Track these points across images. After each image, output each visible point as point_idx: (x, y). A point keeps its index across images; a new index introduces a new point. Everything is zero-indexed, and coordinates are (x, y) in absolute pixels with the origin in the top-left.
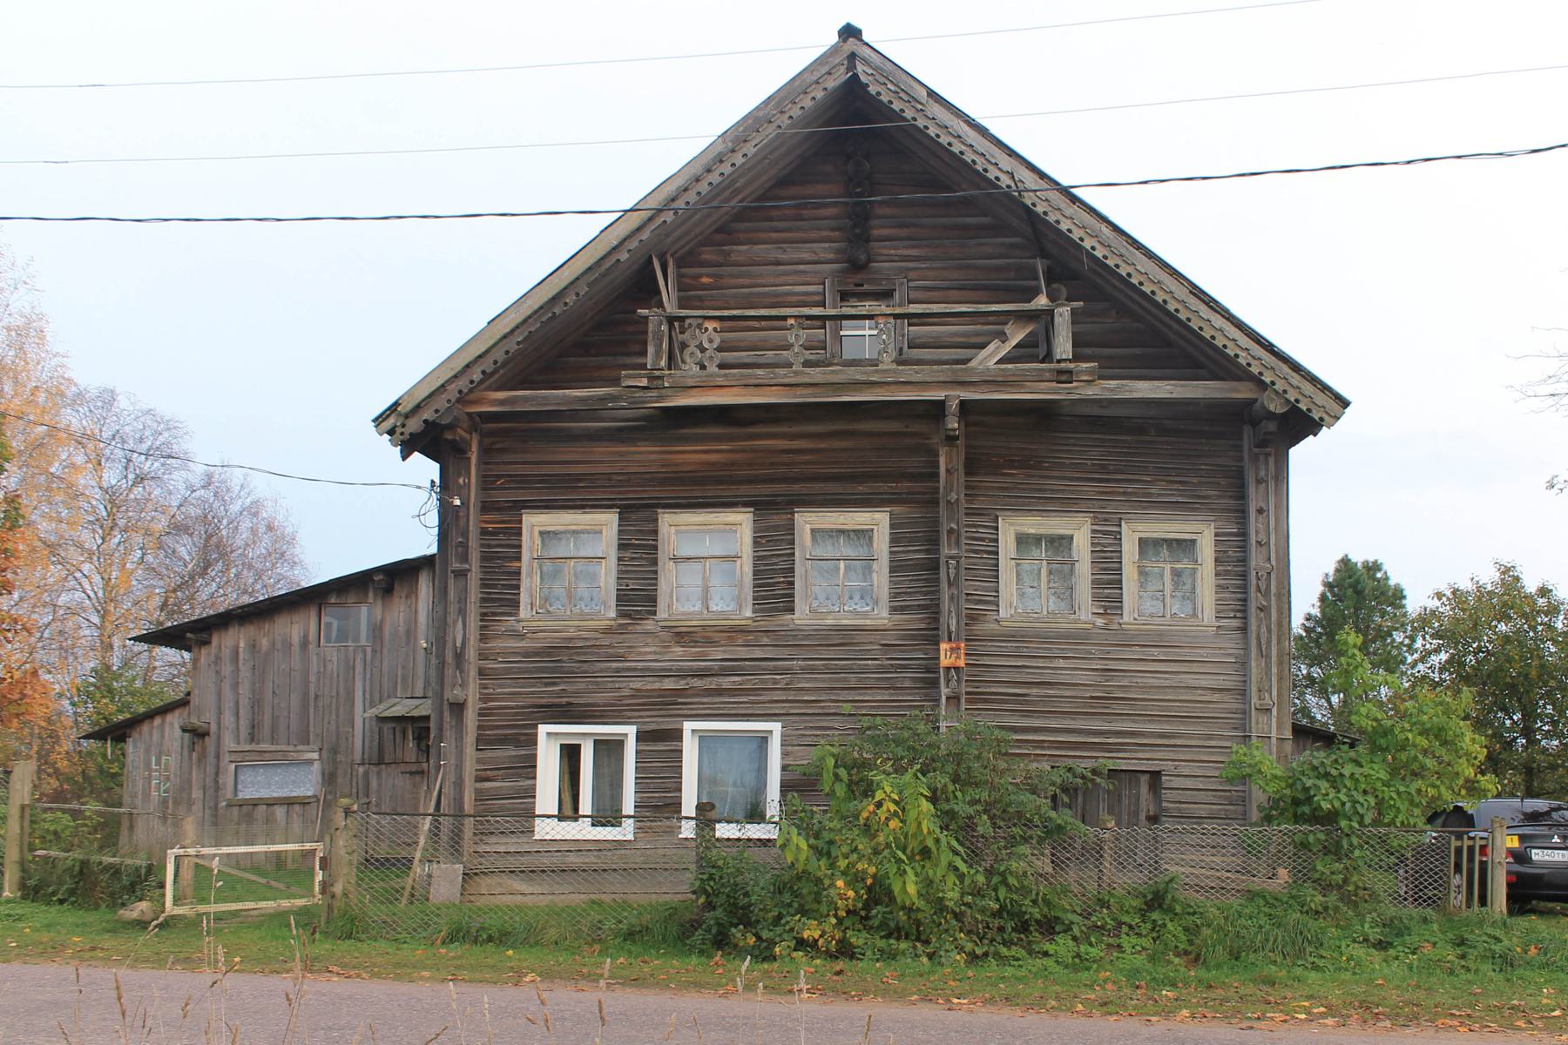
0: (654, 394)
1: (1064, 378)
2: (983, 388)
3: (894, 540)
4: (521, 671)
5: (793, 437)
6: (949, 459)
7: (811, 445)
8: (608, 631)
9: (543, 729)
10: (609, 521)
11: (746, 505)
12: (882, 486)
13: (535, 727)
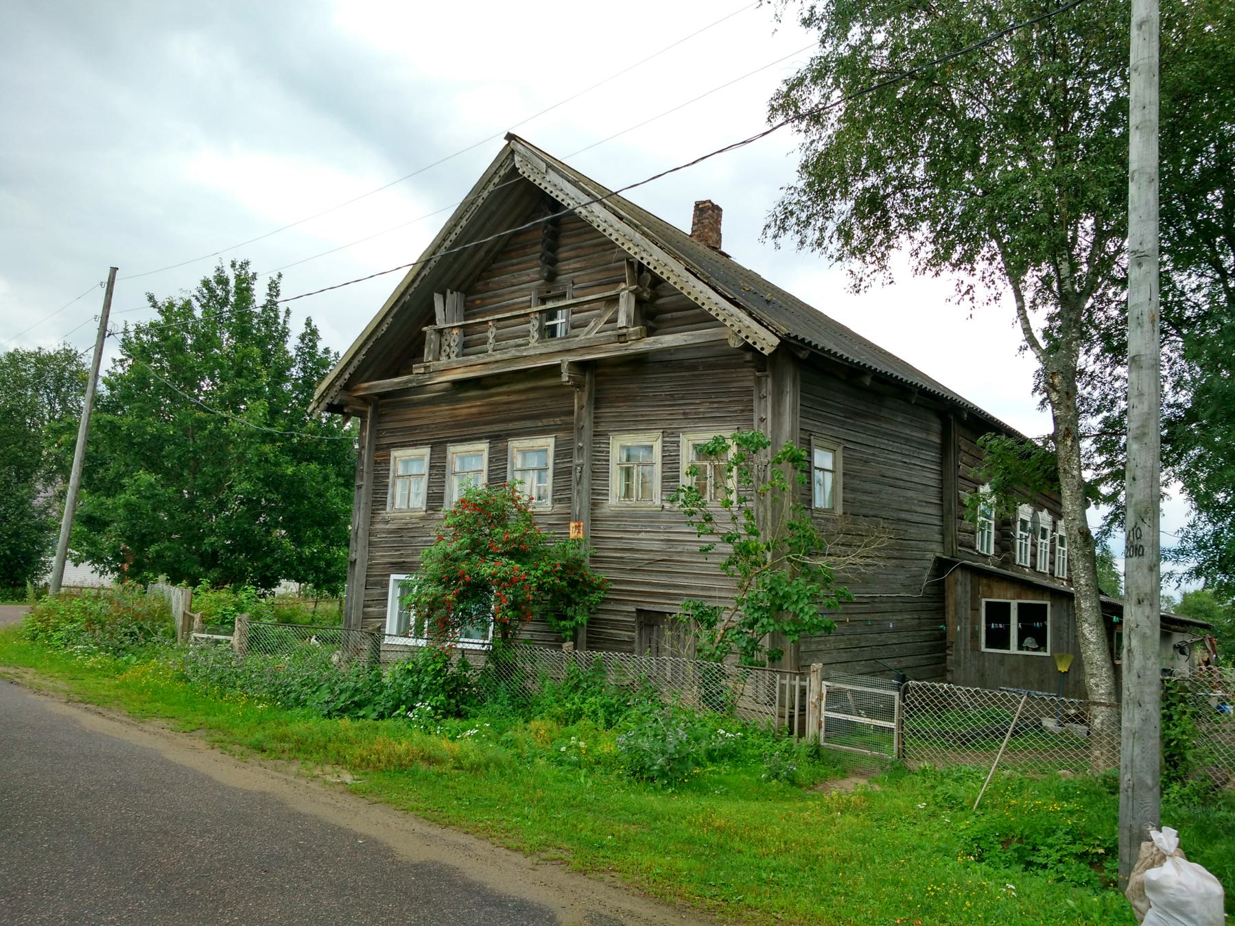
0: (427, 376)
1: (622, 339)
2: (582, 351)
3: (556, 455)
4: (386, 542)
5: (508, 393)
6: (580, 399)
7: (524, 397)
8: (422, 519)
9: (393, 577)
10: (426, 451)
11: (487, 438)
12: (550, 421)
13: (389, 576)
